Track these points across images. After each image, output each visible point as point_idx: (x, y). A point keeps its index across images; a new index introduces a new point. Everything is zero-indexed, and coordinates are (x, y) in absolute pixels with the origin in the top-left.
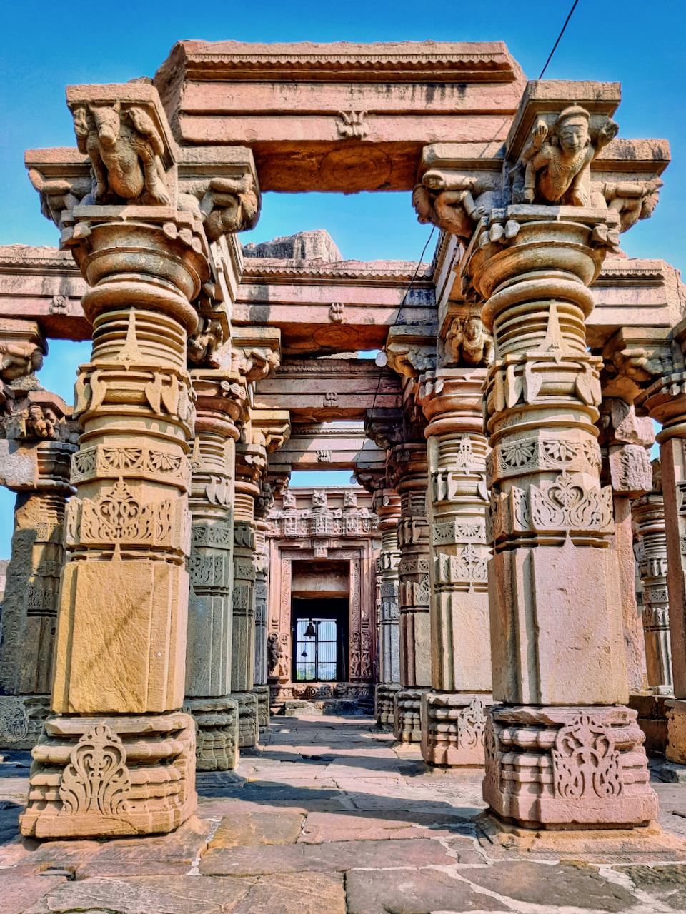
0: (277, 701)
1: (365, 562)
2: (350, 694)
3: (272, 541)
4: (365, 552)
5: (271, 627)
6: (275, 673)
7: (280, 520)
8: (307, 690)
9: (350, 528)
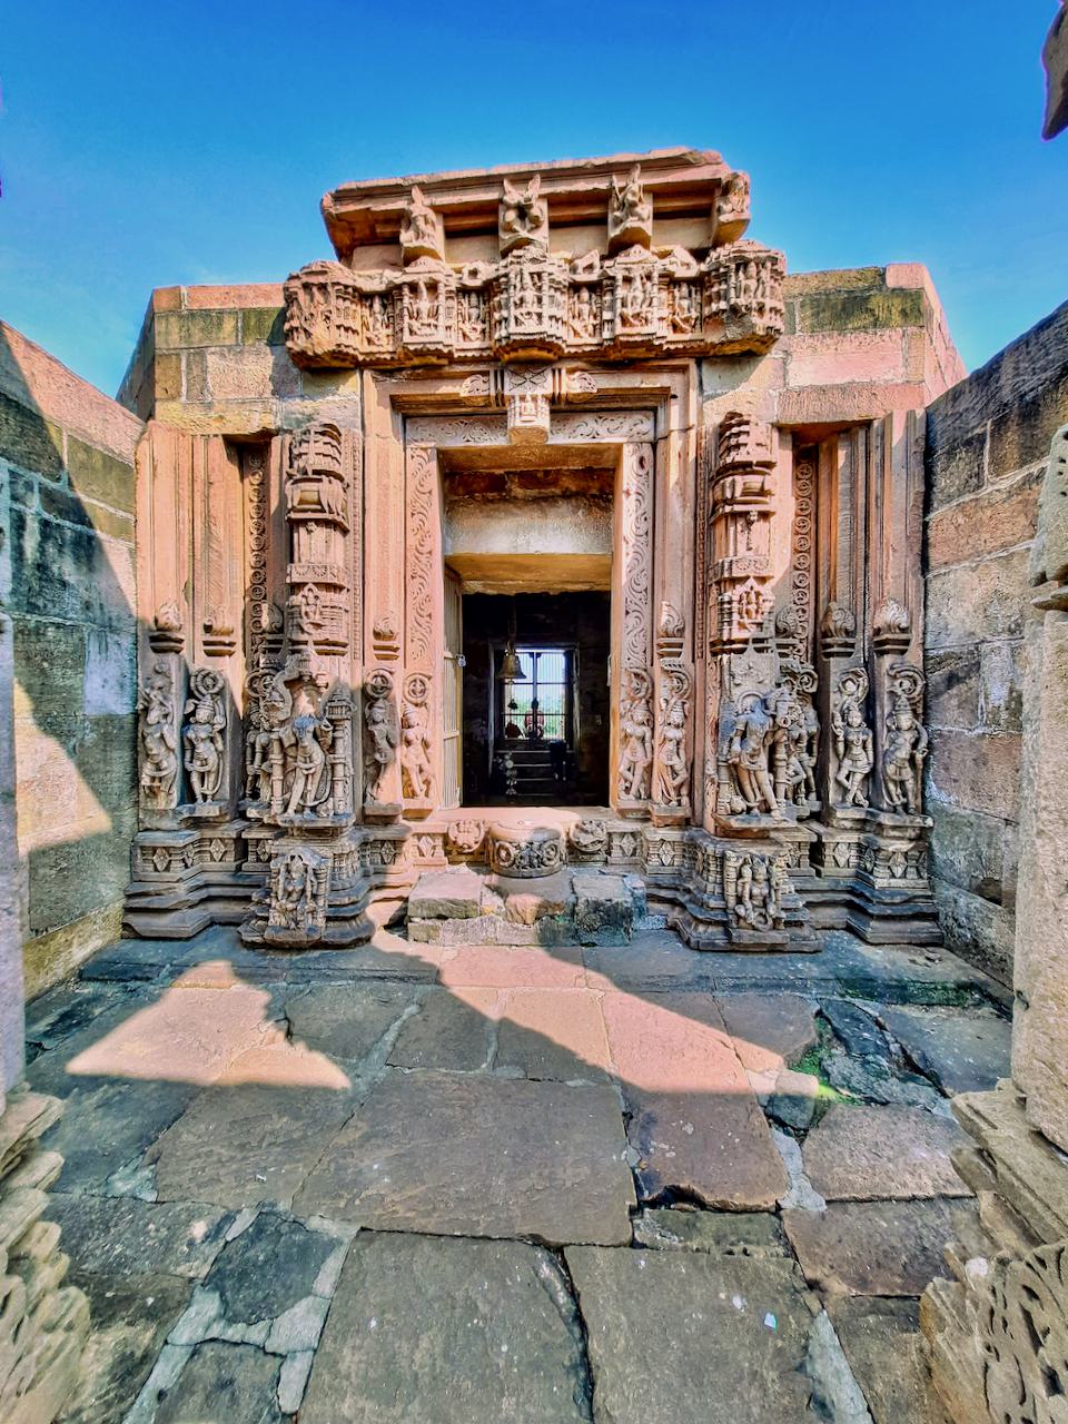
0: (391, 880)
1: (676, 442)
2: (616, 852)
3: (368, 374)
4: (675, 408)
5: (370, 653)
6: (389, 792)
7: (390, 296)
8: (485, 840)
9: (629, 311)
